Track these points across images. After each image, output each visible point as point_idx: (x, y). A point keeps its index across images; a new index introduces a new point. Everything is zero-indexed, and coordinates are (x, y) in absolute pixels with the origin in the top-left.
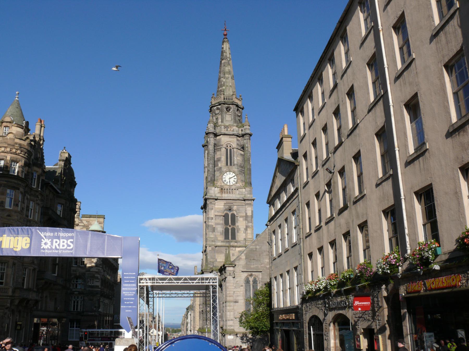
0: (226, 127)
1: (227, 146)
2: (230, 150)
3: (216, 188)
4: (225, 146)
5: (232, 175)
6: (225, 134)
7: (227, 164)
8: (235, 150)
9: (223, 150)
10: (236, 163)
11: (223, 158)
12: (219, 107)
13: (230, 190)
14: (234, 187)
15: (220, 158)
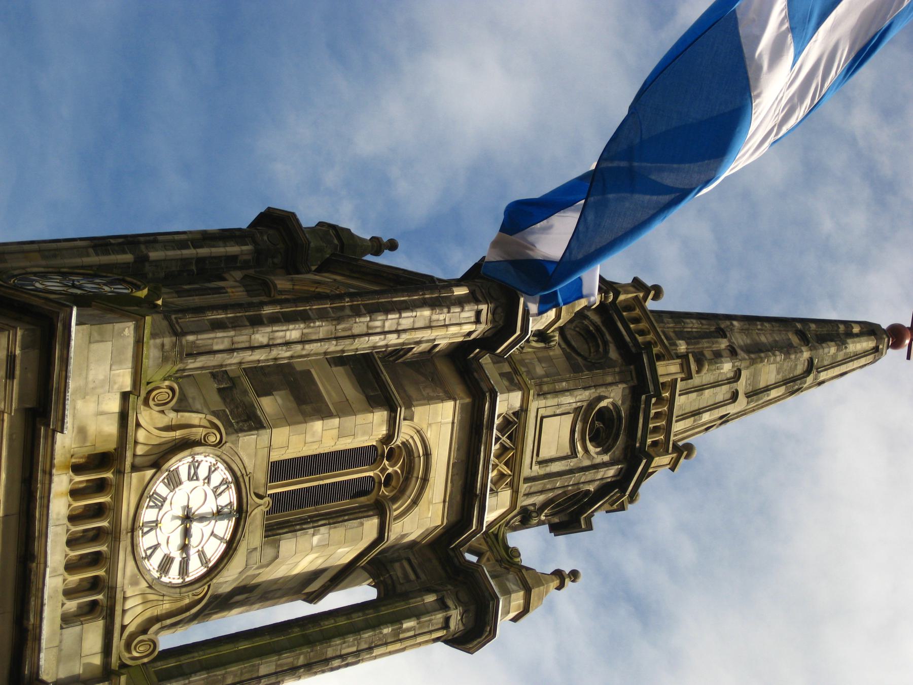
0: (514, 425)
1: (391, 455)
2: (361, 489)
3: (113, 405)
4: (405, 433)
5: (210, 540)
6: (473, 430)
7: (280, 470)
8: (371, 526)
9: (368, 429)
10: (287, 544)
11: (322, 436)
12: (613, 354)
13: (103, 534)
14: (125, 568)
15: (324, 413)
